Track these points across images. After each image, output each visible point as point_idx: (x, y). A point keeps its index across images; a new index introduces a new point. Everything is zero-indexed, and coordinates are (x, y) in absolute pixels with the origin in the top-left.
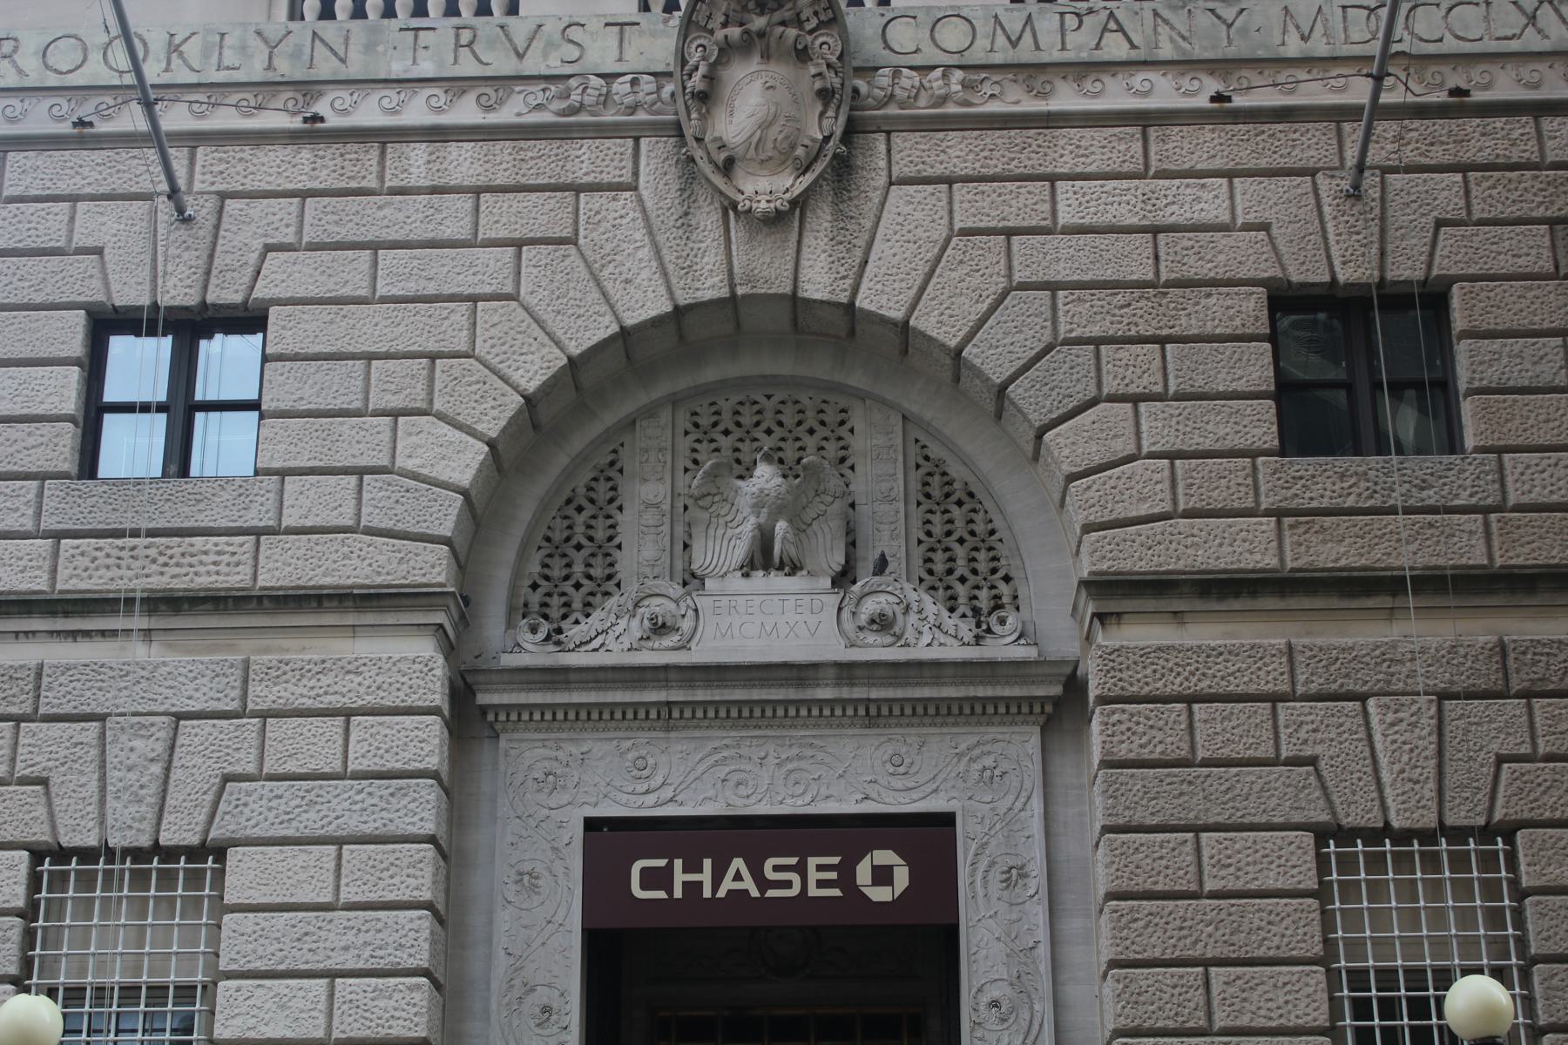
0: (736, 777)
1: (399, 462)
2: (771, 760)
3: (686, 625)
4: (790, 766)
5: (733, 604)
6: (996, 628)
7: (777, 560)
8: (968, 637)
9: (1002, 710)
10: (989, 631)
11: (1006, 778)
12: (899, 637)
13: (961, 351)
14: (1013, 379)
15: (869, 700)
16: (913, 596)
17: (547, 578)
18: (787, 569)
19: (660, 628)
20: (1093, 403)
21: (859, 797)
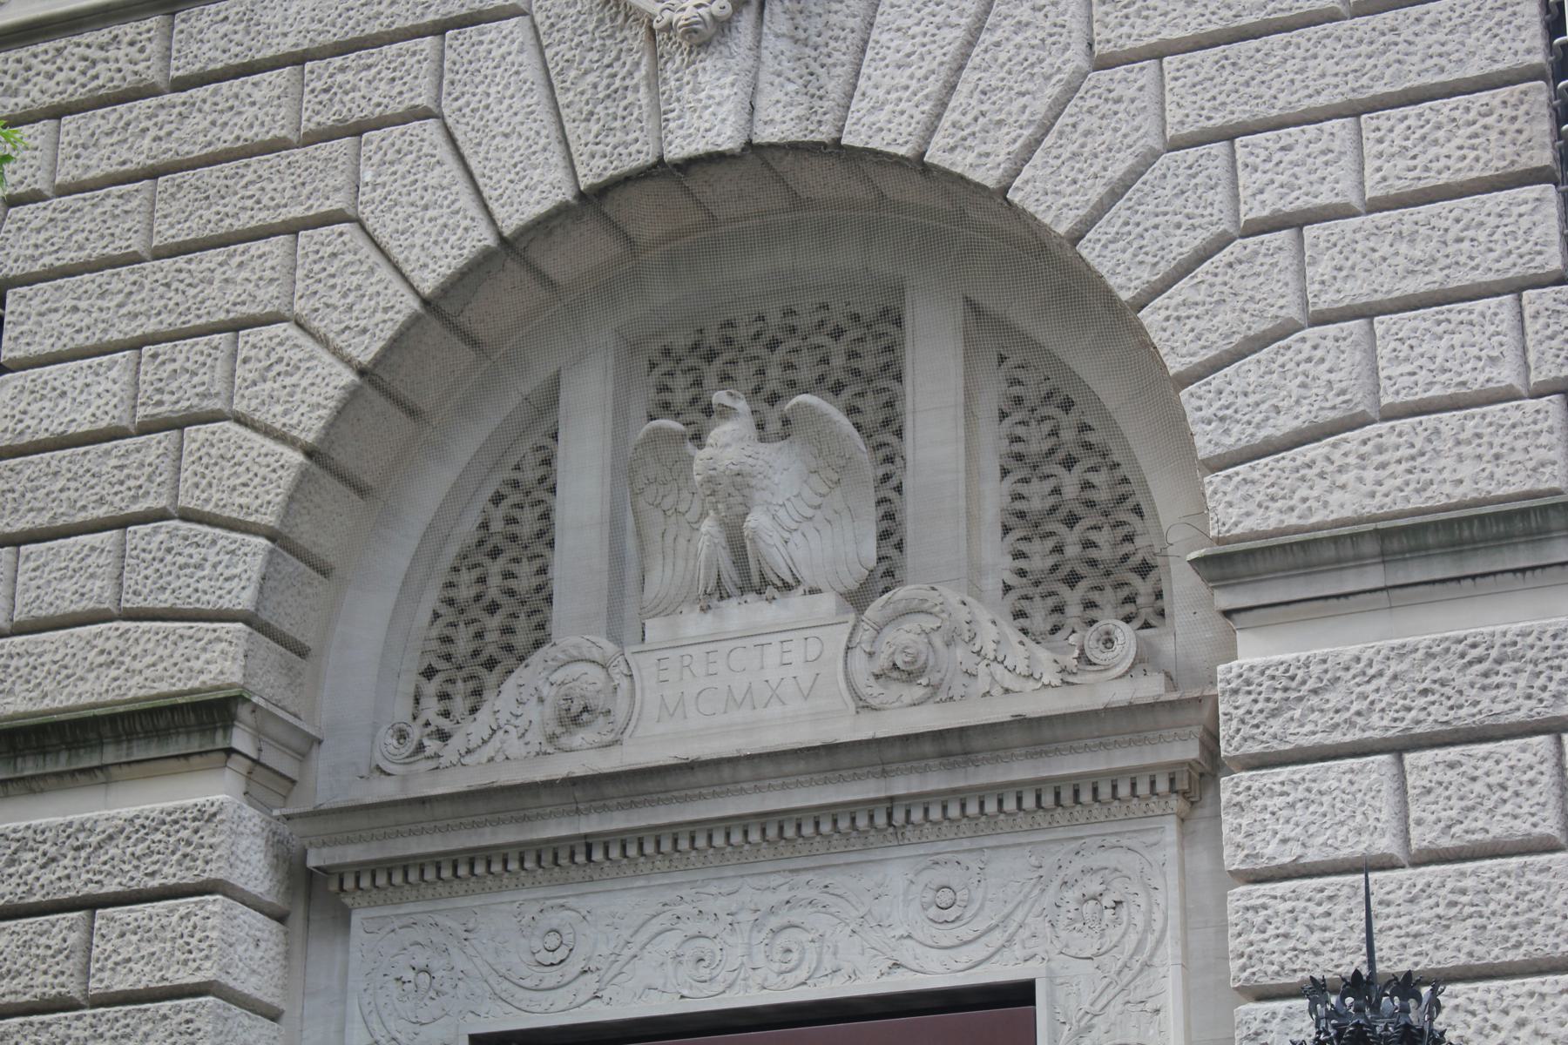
0: (690, 950)
1: (184, 501)
2: (746, 917)
3: (621, 708)
4: (774, 922)
5: (687, 660)
6: (1096, 654)
7: (756, 579)
8: (1051, 677)
9: (1029, 802)
10: (1083, 658)
11: (1123, 912)
12: (934, 688)
13: (1005, 190)
14: (1089, 222)
15: (892, 799)
16: (963, 614)
17: (448, 657)
18: (770, 591)
19: (574, 717)
20: (1222, 242)
21: (884, 967)
